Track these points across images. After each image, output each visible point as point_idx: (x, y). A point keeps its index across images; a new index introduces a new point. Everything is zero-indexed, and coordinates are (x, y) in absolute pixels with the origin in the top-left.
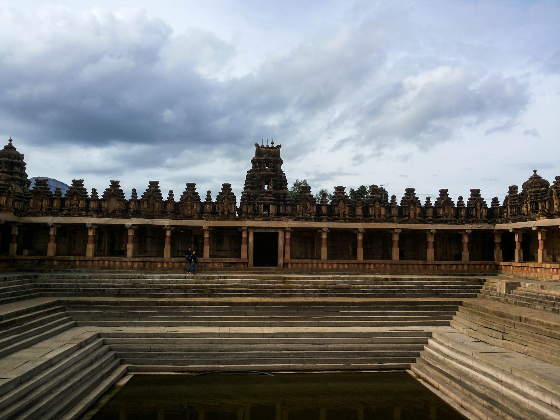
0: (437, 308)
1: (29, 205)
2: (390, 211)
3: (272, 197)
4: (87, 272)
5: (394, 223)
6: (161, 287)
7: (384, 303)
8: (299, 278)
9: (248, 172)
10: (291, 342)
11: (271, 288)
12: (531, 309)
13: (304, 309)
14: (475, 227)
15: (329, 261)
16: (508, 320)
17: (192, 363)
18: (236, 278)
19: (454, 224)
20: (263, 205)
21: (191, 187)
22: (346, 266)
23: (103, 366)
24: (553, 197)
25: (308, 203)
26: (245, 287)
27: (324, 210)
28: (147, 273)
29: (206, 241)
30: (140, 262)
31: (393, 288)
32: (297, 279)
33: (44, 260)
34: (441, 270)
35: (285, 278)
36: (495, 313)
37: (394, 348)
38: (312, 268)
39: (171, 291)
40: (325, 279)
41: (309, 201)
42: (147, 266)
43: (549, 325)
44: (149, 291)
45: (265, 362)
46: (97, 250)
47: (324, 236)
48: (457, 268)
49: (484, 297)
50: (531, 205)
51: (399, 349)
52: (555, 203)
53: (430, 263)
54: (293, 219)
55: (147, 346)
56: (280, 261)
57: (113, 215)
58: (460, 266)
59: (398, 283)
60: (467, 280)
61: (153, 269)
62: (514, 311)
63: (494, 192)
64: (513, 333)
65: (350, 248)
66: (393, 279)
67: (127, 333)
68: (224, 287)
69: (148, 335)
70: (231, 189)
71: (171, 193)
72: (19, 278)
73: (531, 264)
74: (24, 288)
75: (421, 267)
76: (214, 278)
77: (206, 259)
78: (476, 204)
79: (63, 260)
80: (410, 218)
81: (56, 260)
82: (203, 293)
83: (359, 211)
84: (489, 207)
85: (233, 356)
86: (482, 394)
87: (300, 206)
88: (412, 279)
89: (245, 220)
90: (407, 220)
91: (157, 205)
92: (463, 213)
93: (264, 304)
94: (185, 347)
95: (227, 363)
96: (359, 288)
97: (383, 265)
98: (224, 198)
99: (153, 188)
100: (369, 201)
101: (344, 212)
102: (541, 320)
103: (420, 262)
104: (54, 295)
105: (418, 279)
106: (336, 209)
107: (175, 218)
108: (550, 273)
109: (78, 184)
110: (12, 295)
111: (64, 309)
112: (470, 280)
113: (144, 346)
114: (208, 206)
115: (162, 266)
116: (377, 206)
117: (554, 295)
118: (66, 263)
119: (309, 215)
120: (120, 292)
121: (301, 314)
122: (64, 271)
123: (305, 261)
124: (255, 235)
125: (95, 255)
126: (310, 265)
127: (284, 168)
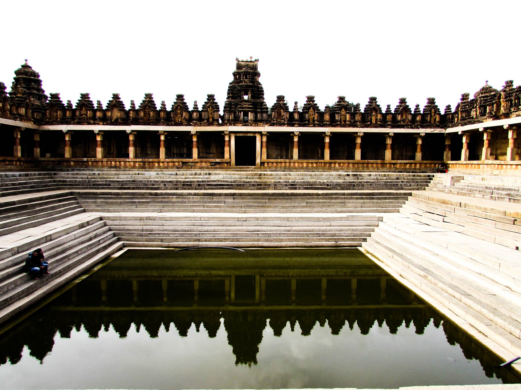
0: (390, 198)
1: (46, 116)
2: (354, 118)
3: (251, 105)
4: (98, 170)
5: (357, 127)
6: (157, 182)
7: (344, 194)
8: (275, 175)
9: (230, 84)
10: (262, 224)
11: (248, 182)
12: (470, 197)
13: (275, 199)
14: (429, 131)
15: (300, 161)
16: (450, 206)
17: (176, 240)
18: (219, 174)
19: (410, 128)
20: (242, 113)
21: (180, 97)
22: (315, 165)
23: (101, 242)
24: (501, 100)
25: (282, 111)
26: (227, 182)
27: (296, 116)
28: (146, 171)
29: (194, 144)
30: (140, 162)
31: (353, 182)
32: (271, 175)
33: (63, 162)
34: (396, 168)
35: (260, 175)
37: (349, 230)
38: (285, 167)
39: (165, 185)
40: (295, 176)
41: (283, 109)
42: (147, 166)
43: (486, 209)
44: (146, 185)
45: (238, 240)
46: (108, 154)
47: (296, 139)
48: (410, 166)
49: (431, 190)
50: (480, 108)
51: (353, 230)
52: (502, 106)
53: (387, 162)
54: (269, 124)
55: (140, 228)
56: (258, 161)
57: (116, 123)
58: (413, 165)
59: (358, 179)
60: (418, 176)
61: (151, 168)
62: (456, 199)
63: (448, 100)
65: (320, 150)
66: (354, 175)
67: (124, 217)
68: (208, 181)
69: (141, 219)
70: (215, 99)
71: (163, 104)
72: (40, 174)
73: (475, 162)
74: (45, 182)
75: (379, 166)
76: (200, 174)
77: (195, 159)
78: (430, 110)
79: (78, 161)
80: (371, 123)
81: (72, 161)
82: (191, 186)
83: (327, 117)
84: (442, 112)
85: (211, 235)
86: (420, 266)
87: (275, 113)
88: (370, 175)
89: (227, 125)
90: (369, 125)
91: (151, 113)
92: (418, 118)
93: (241, 195)
94: (171, 228)
95: (206, 241)
96: (324, 182)
97: (347, 164)
98: (209, 107)
99: (148, 99)
100: (336, 108)
101: (314, 118)
102: (479, 205)
103: (379, 161)
104: (70, 189)
105: (376, 175)
106: (307, 115)
107: (168, 125)
108: (491, 168)
109: (85, 97)
110: (31, 187)
111: (75, 199)
112: (420, 176)
113: (136, 228)
114: (195, 114)
115: (159, 165)
116: (343, 113)
118: (81, 163)
119: (283, 121)
120: (123, 185)
121: (272, 202)
122: (79, 170)
123: (279, 160)
124: (236, 138)
125: (104, 156)
126: (283, 164)
127: (261, 80)
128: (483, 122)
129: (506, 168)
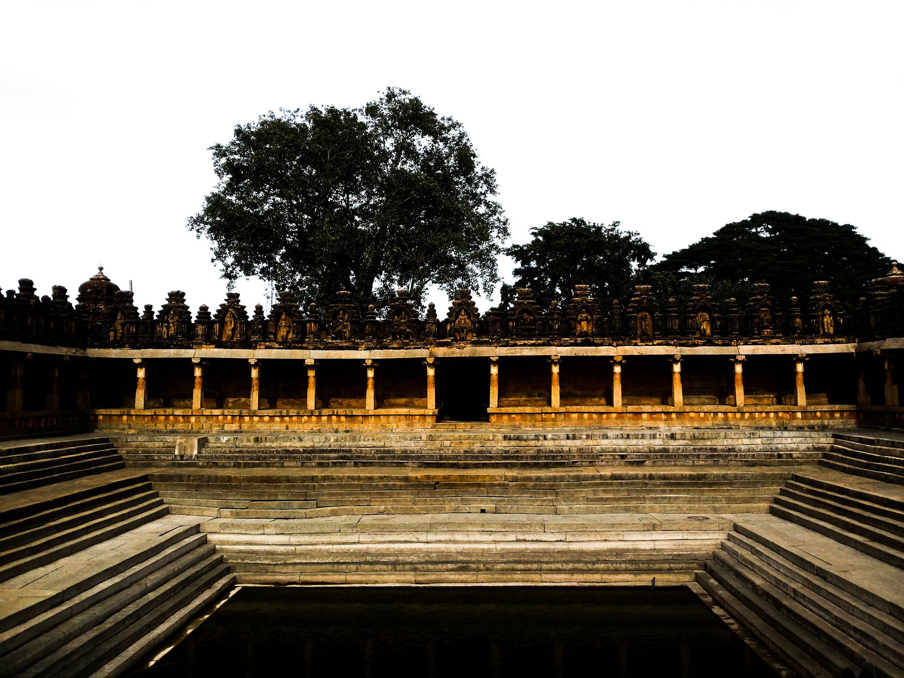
10: (97, 598)
64: (326, 498)
105: (47, 447)
128: (192, 348)
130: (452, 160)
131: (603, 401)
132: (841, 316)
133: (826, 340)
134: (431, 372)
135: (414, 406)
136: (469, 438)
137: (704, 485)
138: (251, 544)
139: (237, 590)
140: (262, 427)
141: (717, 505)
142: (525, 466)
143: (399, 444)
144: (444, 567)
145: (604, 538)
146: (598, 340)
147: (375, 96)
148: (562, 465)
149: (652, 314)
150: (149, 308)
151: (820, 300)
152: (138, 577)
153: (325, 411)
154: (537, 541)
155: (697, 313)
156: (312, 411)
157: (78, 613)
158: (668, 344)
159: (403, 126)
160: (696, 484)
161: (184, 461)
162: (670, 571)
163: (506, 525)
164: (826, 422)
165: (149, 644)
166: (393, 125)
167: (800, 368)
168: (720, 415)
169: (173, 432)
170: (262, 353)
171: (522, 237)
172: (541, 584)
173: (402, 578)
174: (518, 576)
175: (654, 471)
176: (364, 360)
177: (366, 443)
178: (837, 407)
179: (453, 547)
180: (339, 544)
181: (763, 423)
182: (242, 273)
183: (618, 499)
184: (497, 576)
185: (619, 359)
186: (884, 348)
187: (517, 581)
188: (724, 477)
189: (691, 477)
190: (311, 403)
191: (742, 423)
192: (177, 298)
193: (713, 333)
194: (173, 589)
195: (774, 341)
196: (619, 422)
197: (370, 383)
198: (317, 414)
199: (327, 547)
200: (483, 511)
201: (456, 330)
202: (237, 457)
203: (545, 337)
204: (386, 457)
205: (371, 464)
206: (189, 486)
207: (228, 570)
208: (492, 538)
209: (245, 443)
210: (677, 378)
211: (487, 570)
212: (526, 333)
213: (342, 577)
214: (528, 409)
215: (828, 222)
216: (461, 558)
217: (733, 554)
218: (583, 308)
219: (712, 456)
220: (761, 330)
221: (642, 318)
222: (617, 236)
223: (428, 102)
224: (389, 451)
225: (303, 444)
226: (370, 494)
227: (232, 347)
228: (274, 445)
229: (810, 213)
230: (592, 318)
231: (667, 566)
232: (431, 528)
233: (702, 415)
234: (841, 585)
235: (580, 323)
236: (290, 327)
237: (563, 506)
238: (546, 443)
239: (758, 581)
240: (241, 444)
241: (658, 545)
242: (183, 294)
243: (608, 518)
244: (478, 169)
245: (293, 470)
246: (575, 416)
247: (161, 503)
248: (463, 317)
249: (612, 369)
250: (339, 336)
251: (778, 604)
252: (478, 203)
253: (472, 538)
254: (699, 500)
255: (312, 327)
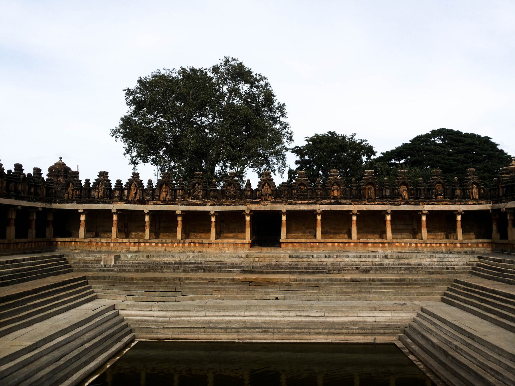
10: (56, 347)
36: (144, 279)
48: (28, 246)
59: (19, 266)
64: (187, 290)
117: (167, 260)
129: (145, 245)
130: (261, 98)
131: (346, 236)
132: (483, 188)
133: (474, 202)
134: (248, 218)
135: (238, 238)
136: (269, 256)
137: (404, 284)
138: (144, 316)
139: (135, 343)
140: (150, 249)
141: (411, 296)
142: (301, 273)
143: (229, 260)
144: (255, 330)
145: (346, 315)
146: (343, 201)
147: (218, 61)
148: (322, 272)
149: (374, 187)
150: (87, 181)
151: (471, 179)
152: (80, 335)
153: (187, 241)
154: (308, 316)
155: (400, 186)
156: (180, 240)
157: (45, 355)
158: (384, 204)
159: (233, 78)
160: (399, 284)
161: (106, 269)
162: (384, 334)
163: (290, 306)
164: (474, 249)
165: (85, 373)
166: (227, 78)
167: (459, 218)
168: (413, 245)
169: (100, 252)
170: (151, 207)
171: (300, 142)
172: (310, 341)
173: (230, 337)
174: (296, 336)
175: (375, 277)
176: (209, 212)
177: (210, 259)
178: (480, 241)
179: (259, 319)
180: (195, 317)
181: (438, 250)
182: (141, 161)
183: (355, 293)
184: (285, 336)
185: (355, 212)
186: (507, 207)
187: (296, 339)
188: (415, 280)
189: (396, 280)
190: (179, 235)
191: (425, 250)
192: (104, 175)
193: (409, 198)
194: (99, 341)
195: (444, 202)
196: (355, 248)
197: (213, 224)
198: (182, 242)
199: (188, 318)
200: (277, 298)
201: (262, 195)
202: (136, 266)
203: (313, 199)
204: (221, 267)
205: (213, 271)
206: (109, 283)
207: (131, 331)
208: (282, 314)
209: (141, 258)
210: (388, 224)
211: (279, 332)
212: (302, 197)
213: (196, 336)
214: (303, 240)
215: (475, 135)
216: (264, 325)
217: (420, 324)
218: (335, 183)
219: (409, 268)
220: (436, 196)
221: (369, 189)
222: (354, 142)
223: (247, 65)
224: (223, 264)
225: (175, 259)
226: (212, 288)
227: (135, 203)
228: (158, 259)
229: (464, 130)
230: (340, 188)
231: (382, 331)
232: (247, 308)
233: (403, 244)
234: (483, 343)
235: (333, 191)
236: (167, 192)
237: (323, 296)
238: (313, 260)
239: (435, 340)
240: (139, 259)
241: (377, 319)
242: (107, 173)
243: (350, 303)
244: (275, 103)
245: (169, 274)
246: (330, 244)
247: (93, 292)
248: (266, 187)
249: (351, 218)
250: (196, 197)
251: (446, 354)
252: (275, 123)
253: (270, 314)
254: (401, 293)
255: (180, 192)
